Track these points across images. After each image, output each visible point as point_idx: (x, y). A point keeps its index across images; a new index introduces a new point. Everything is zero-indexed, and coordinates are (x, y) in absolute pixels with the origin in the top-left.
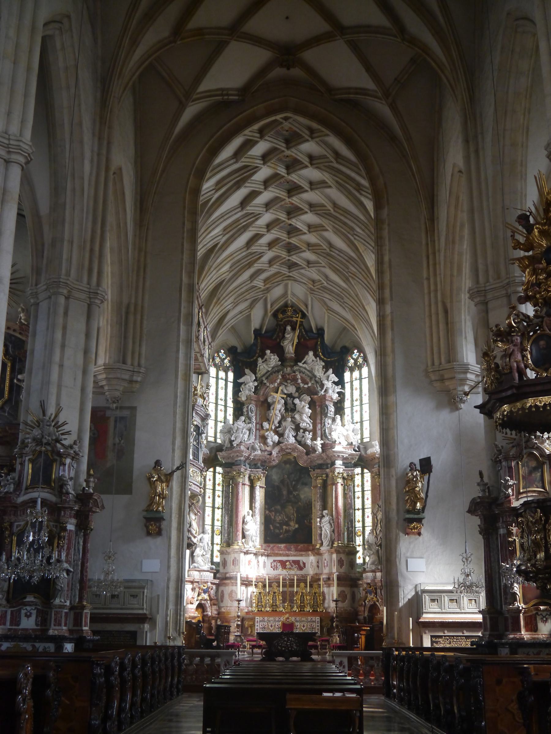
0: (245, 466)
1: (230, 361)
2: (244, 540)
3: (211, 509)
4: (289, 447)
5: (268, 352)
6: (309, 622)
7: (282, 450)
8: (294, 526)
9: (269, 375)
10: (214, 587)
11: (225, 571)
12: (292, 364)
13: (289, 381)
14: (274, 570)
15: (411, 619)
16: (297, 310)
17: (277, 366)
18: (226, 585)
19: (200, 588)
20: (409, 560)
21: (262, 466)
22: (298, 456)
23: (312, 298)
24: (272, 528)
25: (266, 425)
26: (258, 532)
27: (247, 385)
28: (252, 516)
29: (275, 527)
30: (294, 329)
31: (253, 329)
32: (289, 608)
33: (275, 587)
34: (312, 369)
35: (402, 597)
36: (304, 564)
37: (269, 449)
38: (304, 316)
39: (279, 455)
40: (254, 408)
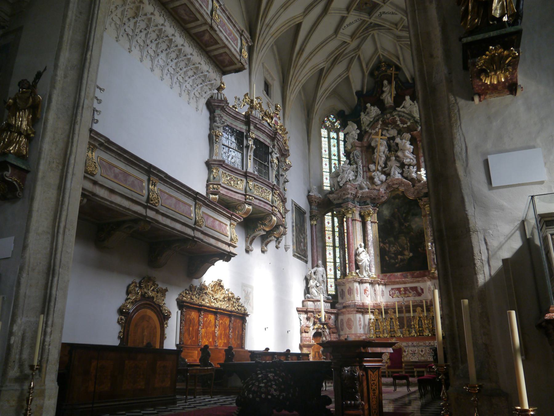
0: (354, 203)
1: (340, 124)
2: (358, 271)
3: (332, 248)
4: (395, 182)
5: (368, 105)
6: (427, 346)
7: (389, 187)
8: (408, 254)
9: (373, 125)
10: (333, 317)
11: (343, 301)
12: (391, 111)
13: (390, 126)
14: (393, 297)
15: (513, 313)
16: (389, 64)
17: (378, 115)
18: (343, 313)
19: (315, 317)
20: (492, 159)
21: (372, 203)
22: (405, 190)
23: (401, 47)
24: (387, 259)
25: (372, 167)
26: (373, 263)
27: (350, 134)
28: (365, 247)
29: (390, 258)
30: (390, 83)
31: (354, 91)
32: (407, 332)
33: (392, 313)
34: (411, 112)
35: (484, 258)
36: (422, 290)
37: (377, 188)
38: (398, 68)
39: (388, 191)
40: (358, 153)
